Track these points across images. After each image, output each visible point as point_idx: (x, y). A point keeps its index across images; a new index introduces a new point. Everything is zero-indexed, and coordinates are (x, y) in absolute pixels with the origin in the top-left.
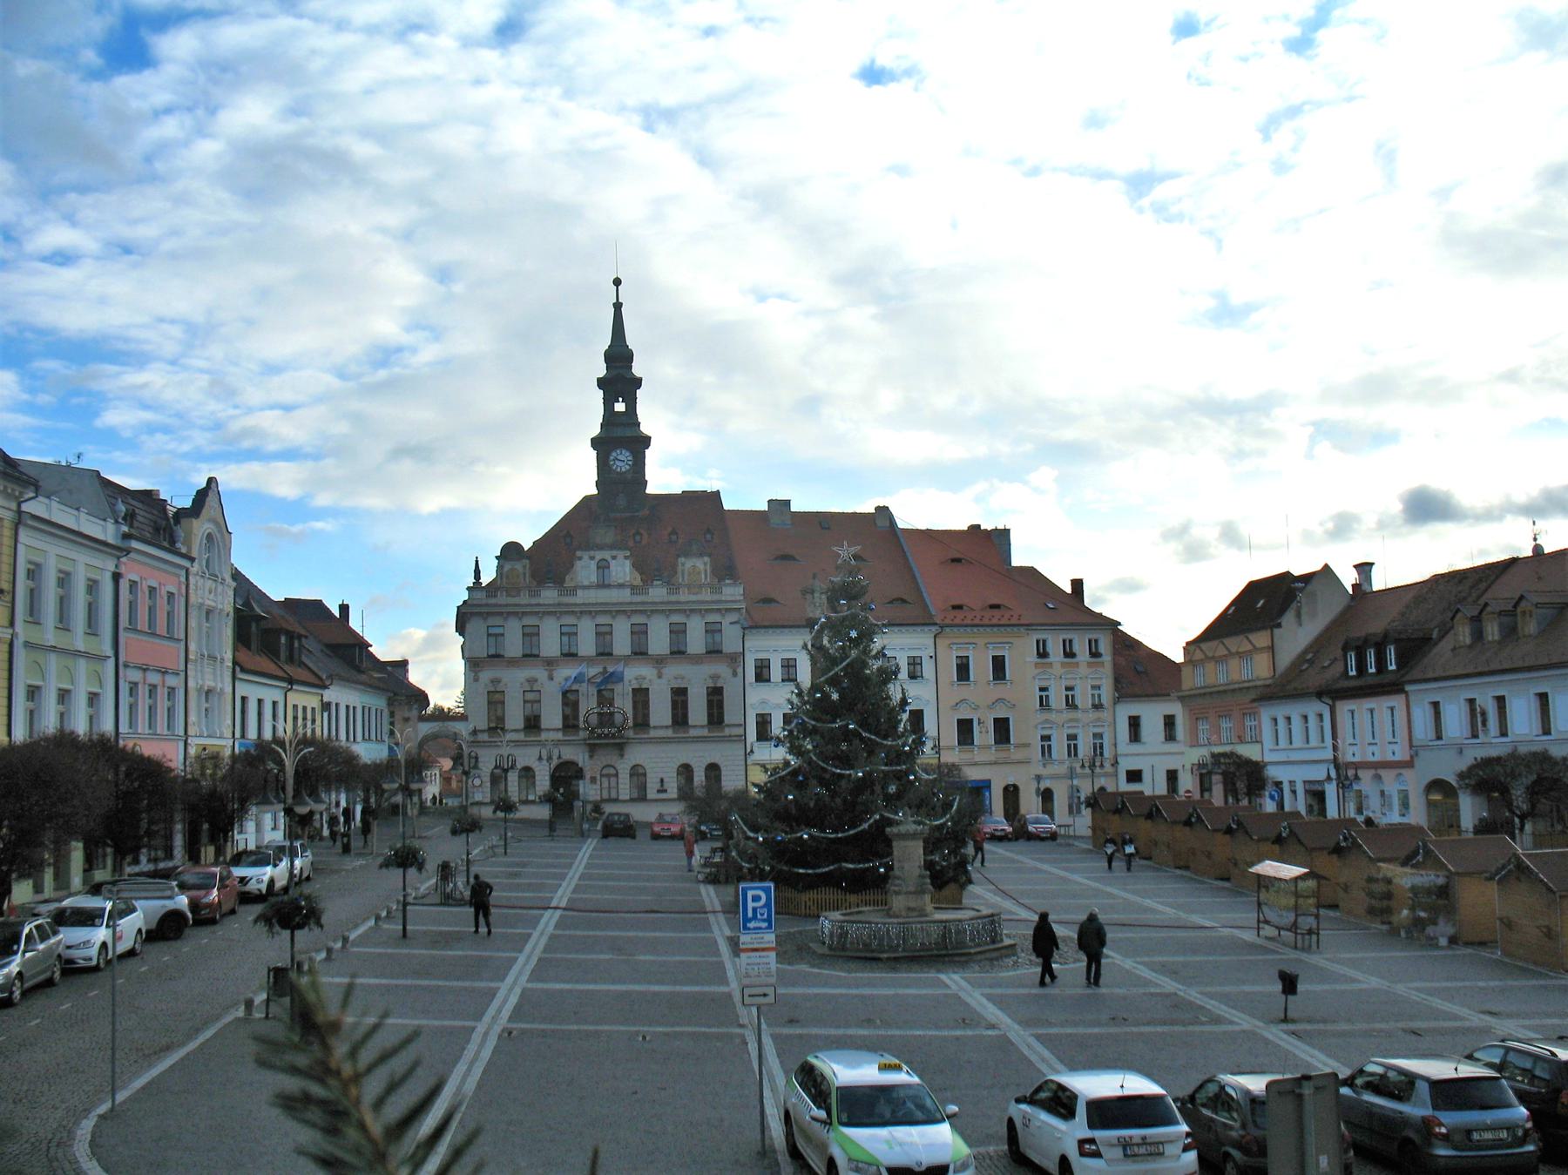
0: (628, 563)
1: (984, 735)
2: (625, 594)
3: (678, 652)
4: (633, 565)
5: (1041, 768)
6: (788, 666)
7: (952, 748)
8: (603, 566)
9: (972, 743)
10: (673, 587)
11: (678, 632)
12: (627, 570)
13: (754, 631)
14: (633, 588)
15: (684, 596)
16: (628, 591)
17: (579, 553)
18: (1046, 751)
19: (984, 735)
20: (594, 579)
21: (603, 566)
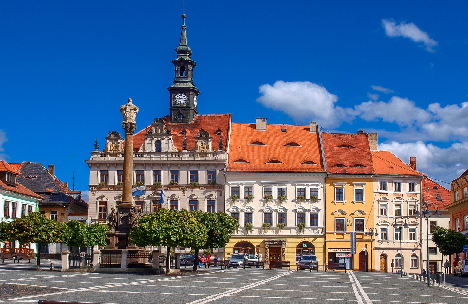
0: (171, 142)
1: (350, 228)
2: (171, 157)
3: (193, 185)
4: (174, 142)
5: (380, 244)
6: (249, 191)
7: (333, 233)
8: (159, 144)
9: (343, 230)
10: (193, 154)
11: (194, 174)
12: (170, 145)
13: (230, 174)
14: (173, 154)
15: (199, 158)
16: (170, 156)
17: (146, 137)
18: (384, 236)
19: (350, 228)
20: (154, 150)
21: (159, 144)
